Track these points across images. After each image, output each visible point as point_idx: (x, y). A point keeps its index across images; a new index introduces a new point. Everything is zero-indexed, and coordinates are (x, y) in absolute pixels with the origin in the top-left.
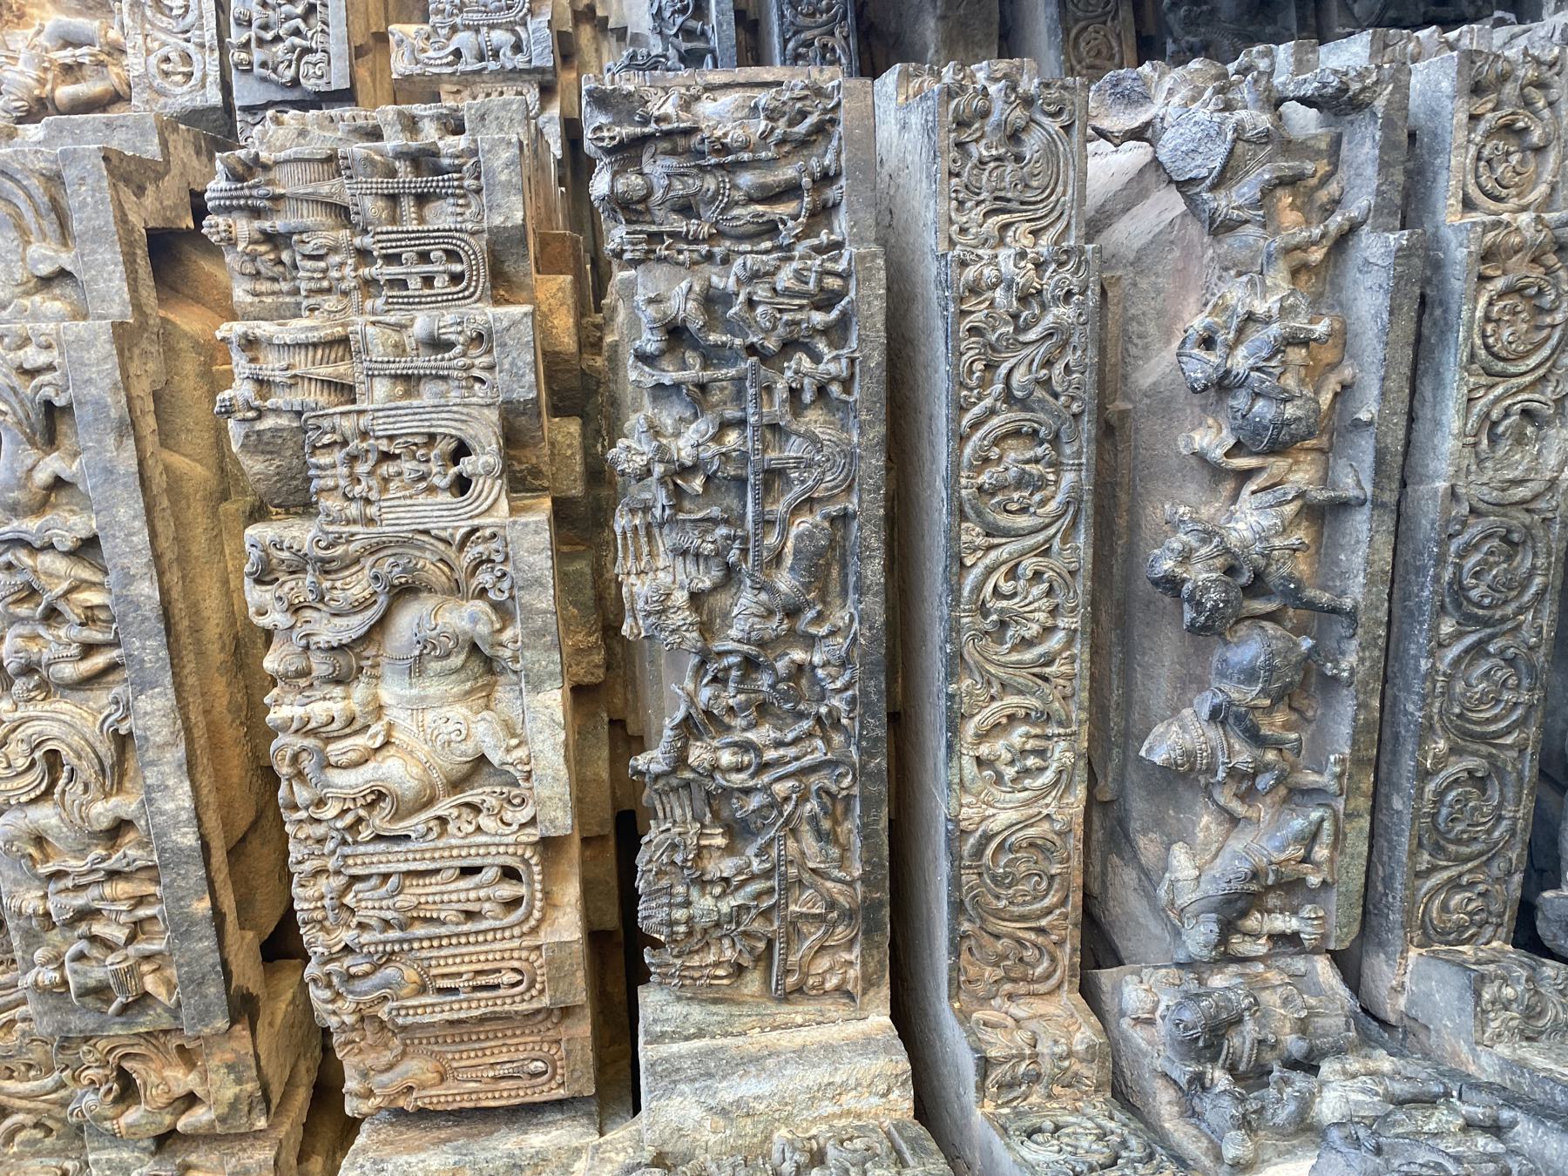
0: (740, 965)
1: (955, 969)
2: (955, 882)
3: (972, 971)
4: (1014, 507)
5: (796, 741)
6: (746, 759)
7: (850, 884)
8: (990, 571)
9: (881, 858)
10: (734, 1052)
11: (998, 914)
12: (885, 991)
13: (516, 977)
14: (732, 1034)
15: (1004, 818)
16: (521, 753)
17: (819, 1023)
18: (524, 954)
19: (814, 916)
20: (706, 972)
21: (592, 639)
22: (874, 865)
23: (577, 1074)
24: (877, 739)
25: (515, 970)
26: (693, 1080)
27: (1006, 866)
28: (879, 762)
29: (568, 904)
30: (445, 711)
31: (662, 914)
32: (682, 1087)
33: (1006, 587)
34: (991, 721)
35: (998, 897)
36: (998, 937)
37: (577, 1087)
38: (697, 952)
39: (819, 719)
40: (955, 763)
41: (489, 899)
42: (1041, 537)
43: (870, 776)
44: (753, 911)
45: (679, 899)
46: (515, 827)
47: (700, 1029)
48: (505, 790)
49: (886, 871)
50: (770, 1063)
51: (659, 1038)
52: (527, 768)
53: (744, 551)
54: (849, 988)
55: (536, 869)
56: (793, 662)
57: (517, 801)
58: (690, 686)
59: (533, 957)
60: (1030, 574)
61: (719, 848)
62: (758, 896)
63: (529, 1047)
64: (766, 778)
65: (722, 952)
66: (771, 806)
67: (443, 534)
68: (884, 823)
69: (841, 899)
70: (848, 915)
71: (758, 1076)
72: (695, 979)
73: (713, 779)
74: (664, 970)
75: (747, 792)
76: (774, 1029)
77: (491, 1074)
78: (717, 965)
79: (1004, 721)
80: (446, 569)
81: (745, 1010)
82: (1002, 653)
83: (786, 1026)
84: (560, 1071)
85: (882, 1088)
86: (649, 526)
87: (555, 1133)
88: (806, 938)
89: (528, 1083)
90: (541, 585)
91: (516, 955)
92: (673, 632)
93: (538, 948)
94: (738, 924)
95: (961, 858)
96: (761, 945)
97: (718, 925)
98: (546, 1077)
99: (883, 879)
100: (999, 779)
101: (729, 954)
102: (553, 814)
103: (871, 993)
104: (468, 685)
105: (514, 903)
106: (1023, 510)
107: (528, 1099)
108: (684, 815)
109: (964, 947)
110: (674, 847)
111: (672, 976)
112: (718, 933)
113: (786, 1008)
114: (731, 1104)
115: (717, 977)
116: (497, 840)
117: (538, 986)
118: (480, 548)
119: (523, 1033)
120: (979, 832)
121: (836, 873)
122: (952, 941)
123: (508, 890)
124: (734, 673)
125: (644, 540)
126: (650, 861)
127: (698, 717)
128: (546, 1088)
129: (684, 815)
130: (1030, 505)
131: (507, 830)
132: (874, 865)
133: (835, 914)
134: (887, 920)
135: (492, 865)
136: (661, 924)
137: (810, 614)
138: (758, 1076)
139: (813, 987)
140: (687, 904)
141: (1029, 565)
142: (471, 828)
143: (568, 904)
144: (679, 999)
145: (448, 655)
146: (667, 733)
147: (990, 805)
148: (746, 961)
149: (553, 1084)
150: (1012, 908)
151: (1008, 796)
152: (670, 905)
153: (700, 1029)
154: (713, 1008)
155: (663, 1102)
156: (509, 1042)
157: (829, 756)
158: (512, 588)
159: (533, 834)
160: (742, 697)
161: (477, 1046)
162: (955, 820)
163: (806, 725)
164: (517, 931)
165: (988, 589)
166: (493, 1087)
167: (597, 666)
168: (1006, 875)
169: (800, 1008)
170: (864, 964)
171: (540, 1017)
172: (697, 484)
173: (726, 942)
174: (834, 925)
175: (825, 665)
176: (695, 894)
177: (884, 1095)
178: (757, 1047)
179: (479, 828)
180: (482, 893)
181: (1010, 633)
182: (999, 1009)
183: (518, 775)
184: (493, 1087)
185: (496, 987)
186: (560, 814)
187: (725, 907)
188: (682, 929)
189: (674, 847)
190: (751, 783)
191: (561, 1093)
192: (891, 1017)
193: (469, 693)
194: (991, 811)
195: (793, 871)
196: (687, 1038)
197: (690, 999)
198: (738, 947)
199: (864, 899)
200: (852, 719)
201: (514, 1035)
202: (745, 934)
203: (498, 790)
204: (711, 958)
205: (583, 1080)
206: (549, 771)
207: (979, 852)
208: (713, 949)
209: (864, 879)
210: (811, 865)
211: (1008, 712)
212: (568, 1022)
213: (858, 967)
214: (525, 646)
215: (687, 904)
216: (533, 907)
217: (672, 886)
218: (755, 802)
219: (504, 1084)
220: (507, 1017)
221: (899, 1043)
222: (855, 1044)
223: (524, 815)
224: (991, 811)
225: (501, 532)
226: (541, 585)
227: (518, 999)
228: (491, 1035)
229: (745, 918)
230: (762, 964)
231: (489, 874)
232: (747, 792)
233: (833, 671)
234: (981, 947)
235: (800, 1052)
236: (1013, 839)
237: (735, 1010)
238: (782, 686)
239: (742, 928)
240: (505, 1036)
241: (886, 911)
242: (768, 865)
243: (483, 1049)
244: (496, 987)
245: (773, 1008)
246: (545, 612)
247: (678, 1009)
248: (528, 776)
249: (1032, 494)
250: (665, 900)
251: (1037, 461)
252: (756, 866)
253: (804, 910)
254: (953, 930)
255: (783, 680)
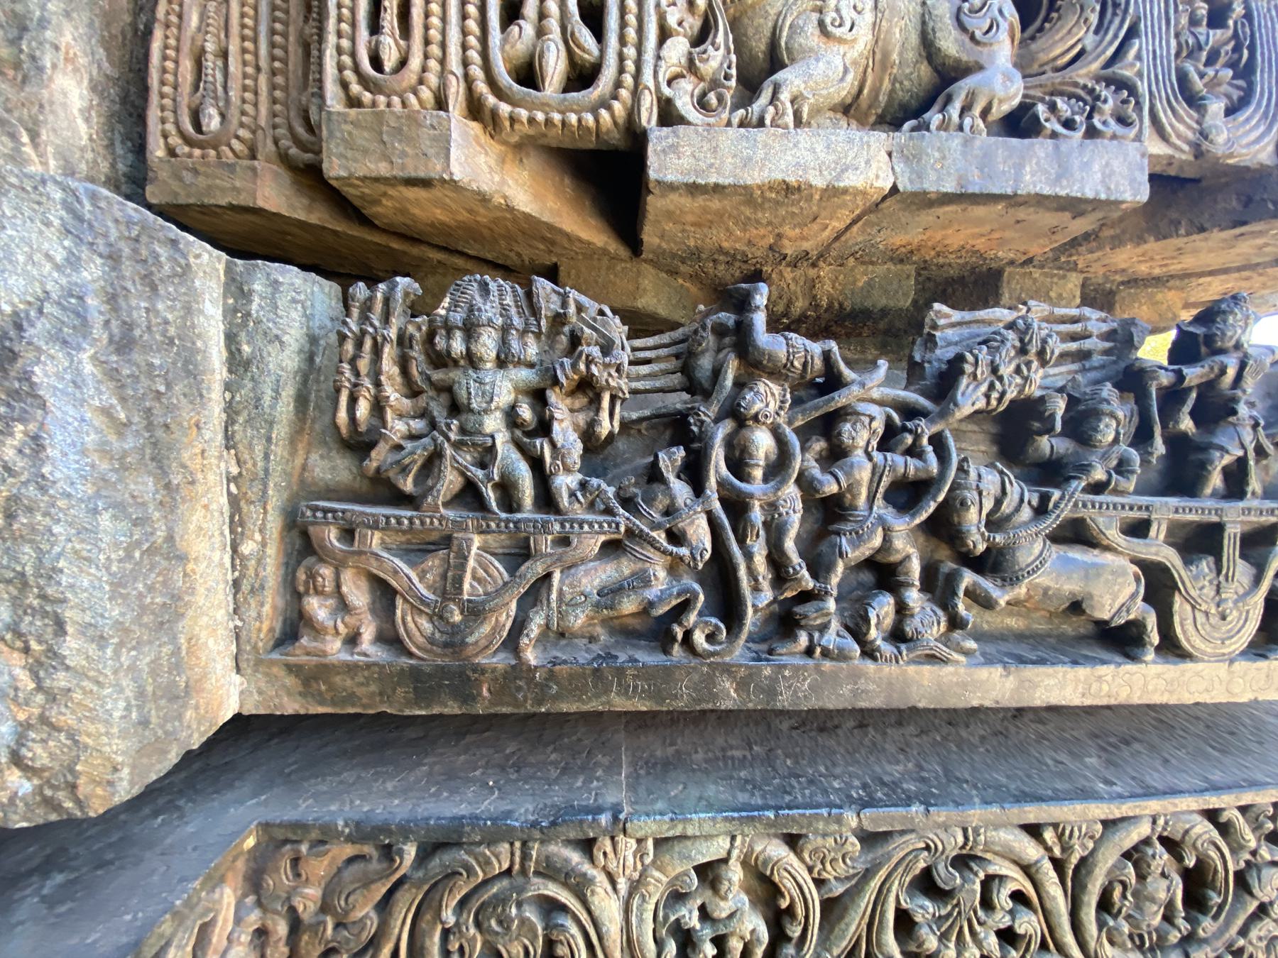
0: (371, 445)
1: (324, 837)
2: (496, 833)
3: (320, 868)
4: (1117, 894)
5: (777, 561)
6: (758, 473)
7: (512, 642)
8: (1028, 870)
9: (556, 698)
10: (187, 415)
11: (427, 907)
12: (291, 706)
13: (390, 58)
14: (230, 422)
15: (608, 907)
16: (789, 119)
17: (236, 584)
18: (433, 79)
19: (459, 581)
20: (367, 382)
21: (824, 303)
22: (544, 686)
23: (188, 177)
24: (772, 692)
25: (403, 63)
26: (112, 299)
27: (524, 921)
28: (729, 695)
29: (503, 182)
30: (869, 17)
31: (489, 310)
32: (92, 272)
33: (1002, 898)
34: (789, 884)
35: (463, 903)
36: (385, 905)
37: (164, 174)
38: (405, 372)
39: (806, 597)
40: (721, 826)
41: (541, 32)
42: (1069, 939)
43: (709, 681)
44: (480, 473)
45: (515, 345)
46: (667, 91)
47: (247, 364)
48: (733, 83)
49: (529, 707)
50: (145, 486)
51: (237, 290)
52: (768, 122)
53: (1098, 488)
54: (304, 641)
55: (589, 119)
56: (908, 557)
57: (712, 98)
58: (876, 394)
59: (426, 94)
60: (1020, 930)
61: (592, 424)
62: (507, 489)
63: (249, 108)
64: (717, 506)
65: (401, 416)
66: (670, 512)
67: (1132, 53)
68: (620, 703)
69: (486, 629)
70: (453, 641)
71: (103, 449)
72: (353, 362)
73: (717, 420)
74: (378, 306)
75: (694, 473)
76: (234, 501)
77: (210, 47)
78: (378, 407)
79: (784, 904)
80: (1061, 62)
81: (279, 450)
82: (898, 895)
83: (237, 523)
84: (197, 152)
85: (38, 754)
86: (1084, 355)
87: (83, 128)
88: (412, 565)
89: (184, 101)
90: (1058, 178)
91: (433, 64)
92: (995, 370)
93: (441, 103)
94: (457, 445)
95: (542, 842)
96: (408, 485)
97: (456, 408)
98: (189, 128)
99: (516, 704)
100: (677, 897)
101: (397, 428)
102: (688, 151)
103: (290, 681)
104: (895, 57)
105: (528, 75)
106: (1105, 904)
107: (154, 99)
108: (639, 378)
109: (368, 849)
110: (607, 349)
111: (364, 318)
112: (439, 412)
113: (274, 523)
114: (26, 377)
115: (353, 400)
116: (649, 56)
117: (367, 97)
118: (1111, 101)
119: (274, 101)
120: (587, 868)
121: (536, 623)
122: (384, 829)
123: (555, 66)
124: (913, 463)
125: (1073, 346)
126: (580, 308)
127: (840, 399)
128: (170, 127)
129: (639, 378)
130: (1115, 917)
131: (662, 79)
132: (544, 686)
133: (457, 618)
134: (436, 710)
135: (602, 52)
136: (471, 310)
137: (987, 584)
138: (103, 449)
139: (312, 576)
140: (502, 362)
141: (1028, 924)
142: (672, 21)
143: (503, 182)
144: (313, 340)
145: (962, 27)
146: (816, 348)
147: (635, 886)
148: (379, 456)
149: (175, 140)
150: (437, 938)
151: (649, 916)
152: (505, 330)
153: (247, 364)
154: (288, 393)
155: (57, 215)
156: (263, 80)
157: (750, 611)
158: (1054, 135)
159: (648, 116)
160: (864, 474)
161: (263, 29)
162: (619, 826)
163: (805, 573)
164: (476, 71)
165: (1001, 867)
166: (186, 47)
167: (790, 303)
168: (504, 922)
169: (272, 550)
170: (351, 669)
171: (300, 130)
172: (1186, 424)
173: (418, 425)
174: (438, 616)
175: (902, 609)
176: (524, 375)
177: (16, 760)
178: (195, 464)
179: (664, 34)
180: (553, 24)
181: (928, 903)
182: (238, 921)
183: (756, 107)
184: (186, 47)
185: (375, 28)
186: (686, 162)
187: (493, 424)
188: (458, 346)
189: (607, 349)
190: (712, 482)
191: (157, 150)
192: (238, 717)
193: (885, 64)
194: (623, 885)
195: (545, 544)
196: (231, 338)
197: (311, 359)
198: (409, 445)
199: (481, 670)
200: (809, 652)
201: (273, 87)
202: (433, 460)
203: (734, 72)
204: (393, 393)
205: (175, 185)
206: (761, 154)
207: (550, 871)
208: (407, 402)
209: (520, 670)
210: (557, 576)
211: (800, 911)
212: (286, 176)
213: (345, 657)
214: (966, 143)
215: (502, 362)
216: (514, 104)
217: (538, 335)
218: (681, 490)
219: (187, 65)
220: (310, 49)
221: (173, 757)
222: (177, 667)
223: (685, 105)
224: (623, 885)
225: (1133, 132)
226: (1058, 178)
227: (346, 59)
228: (278, 52)
229: (466, 459)
230: (364, 486)
231: (585, 36)
232: (694, 473)
233: (888, 622)
234: (367, 883)
235: (172, 553)
236: (574, 930)
237: (281, 431)
238: (877, 541)
239: (449, 451)
240: (273, 73)
241: (452, 708)
242: (565, 501)
243: (255, 41)
244: (375, 28)
245: (275, 500)
246: (1017, 180)
247: (294, 336)
248: (741, 125)
249: (1128, 917)
250: (517, 322)
251: (1168, 918)
252: (565, 482)
253: (471, 563)
254: (405, 832)
255: (887, 539)
